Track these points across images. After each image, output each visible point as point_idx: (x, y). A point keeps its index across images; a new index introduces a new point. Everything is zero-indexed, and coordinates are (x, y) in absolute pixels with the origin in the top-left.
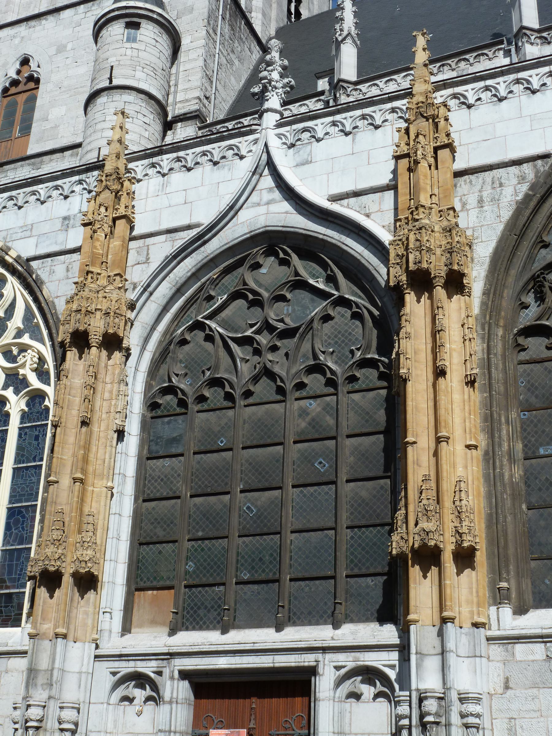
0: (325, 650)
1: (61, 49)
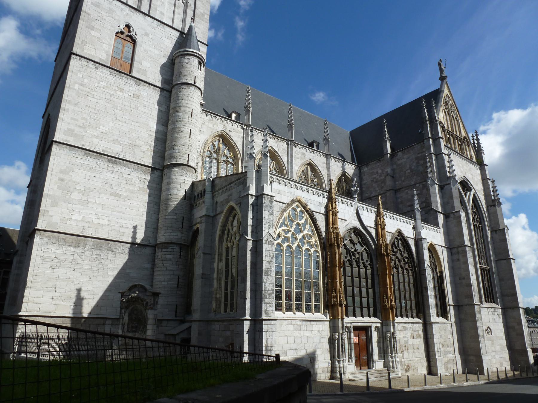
0: (373, 323)
1: (147, 34)
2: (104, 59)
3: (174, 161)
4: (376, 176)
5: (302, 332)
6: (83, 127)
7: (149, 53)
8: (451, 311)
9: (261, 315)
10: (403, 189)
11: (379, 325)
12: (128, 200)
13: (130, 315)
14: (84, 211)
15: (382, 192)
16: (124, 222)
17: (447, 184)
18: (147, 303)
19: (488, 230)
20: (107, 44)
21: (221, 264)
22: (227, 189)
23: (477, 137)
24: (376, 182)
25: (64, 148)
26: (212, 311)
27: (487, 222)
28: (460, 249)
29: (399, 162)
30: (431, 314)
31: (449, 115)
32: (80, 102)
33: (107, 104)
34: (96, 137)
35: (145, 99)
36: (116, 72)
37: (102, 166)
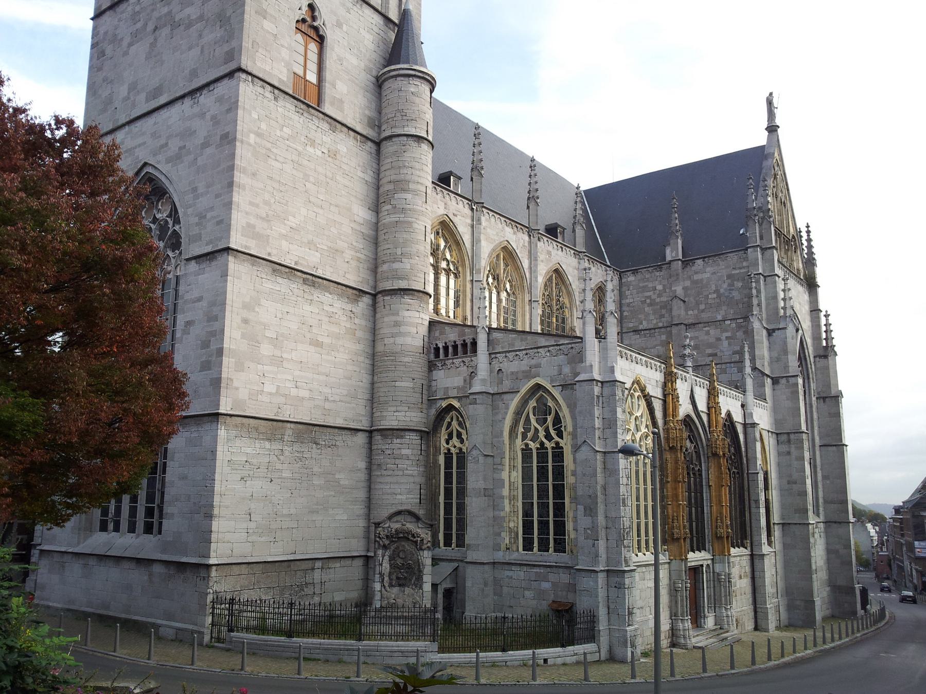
1: (339, 25)
2: (285, 79)
3: (403, 284)
4: (651, 293)
5: (646, 581)
6: (266, 219)
7: (344, 63)
8: (777, 532)
9: (619, 563)
10: (700, 325)
11: (709, 562)
12: (333, 352)
13: (391, 559)
14: (279, 376)
15: (660, 325)
16: (329, 391)
17: (779, 329)
18: (422, 540)
19: (814, 396)
20: (287, 48)
21: (514, 474)
22: (527, 354)
23: (808, 236)
24: (650, 305)
25: (244, 260)
26: (503, 547)
27: (813, 382)
28: (792, 436)
29: (696, 277)
30: (763, 542)
31: (776, 198)
32: (260, 171)
33: (294, 172)
34: (285, 237)
35: (345, 160)
36: (303, 106)
37: (295, 291)
